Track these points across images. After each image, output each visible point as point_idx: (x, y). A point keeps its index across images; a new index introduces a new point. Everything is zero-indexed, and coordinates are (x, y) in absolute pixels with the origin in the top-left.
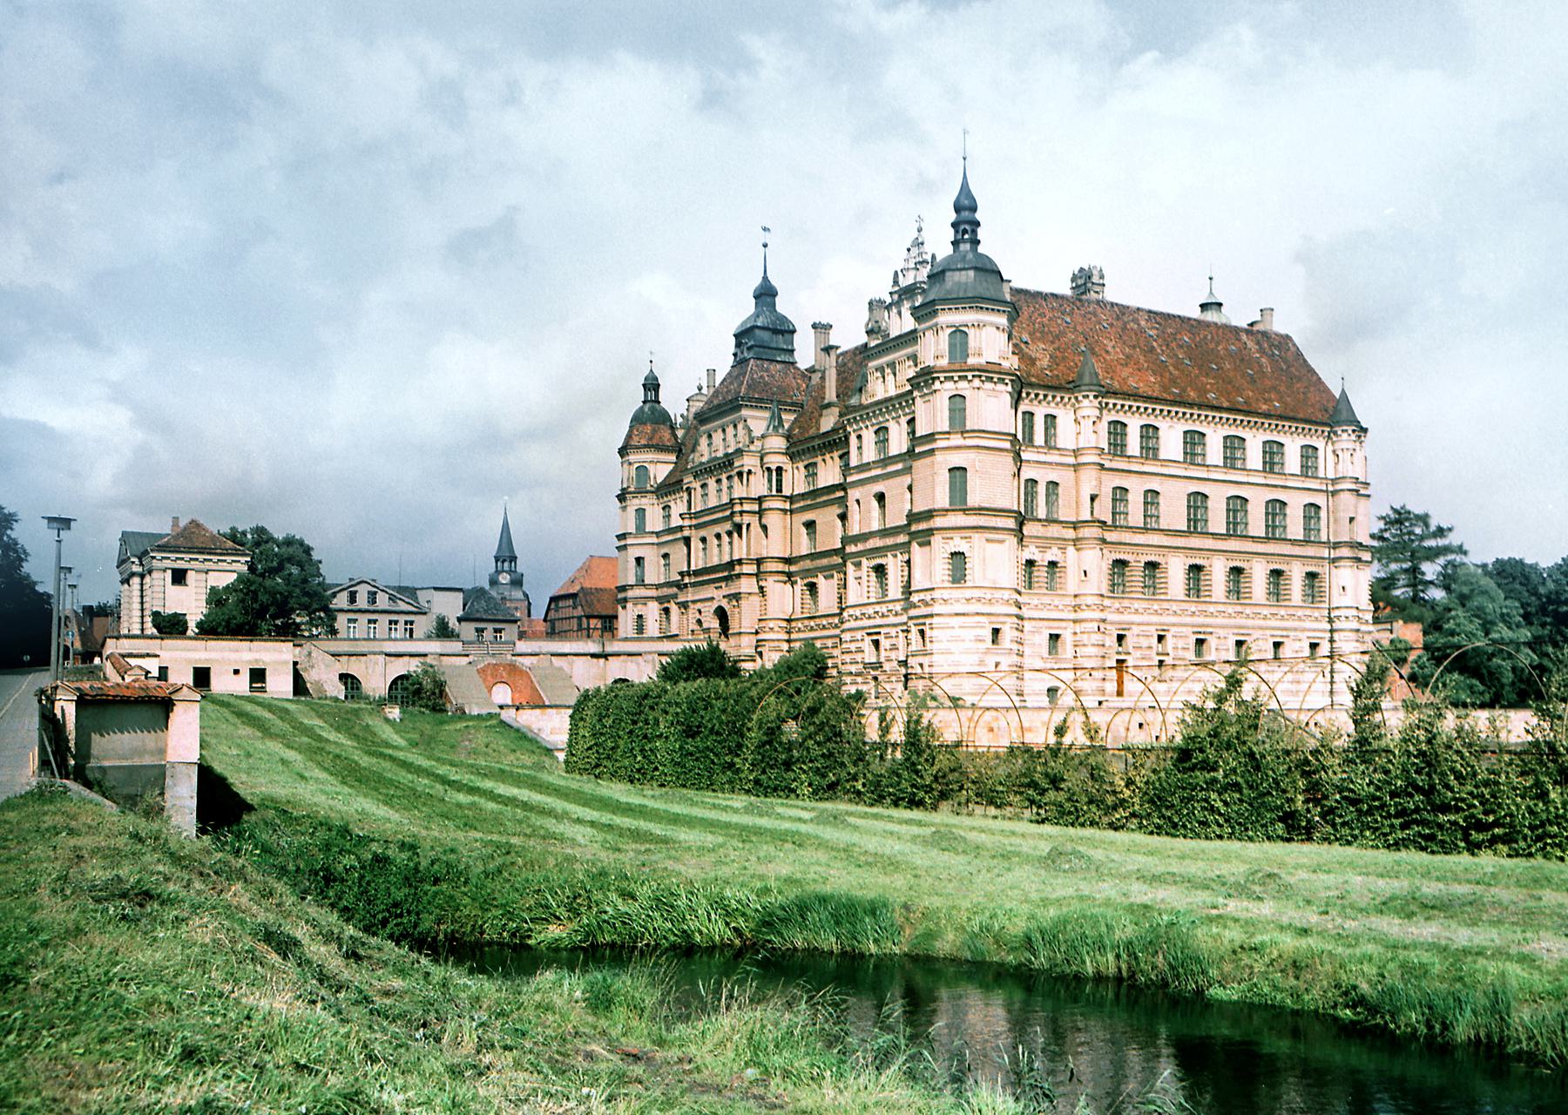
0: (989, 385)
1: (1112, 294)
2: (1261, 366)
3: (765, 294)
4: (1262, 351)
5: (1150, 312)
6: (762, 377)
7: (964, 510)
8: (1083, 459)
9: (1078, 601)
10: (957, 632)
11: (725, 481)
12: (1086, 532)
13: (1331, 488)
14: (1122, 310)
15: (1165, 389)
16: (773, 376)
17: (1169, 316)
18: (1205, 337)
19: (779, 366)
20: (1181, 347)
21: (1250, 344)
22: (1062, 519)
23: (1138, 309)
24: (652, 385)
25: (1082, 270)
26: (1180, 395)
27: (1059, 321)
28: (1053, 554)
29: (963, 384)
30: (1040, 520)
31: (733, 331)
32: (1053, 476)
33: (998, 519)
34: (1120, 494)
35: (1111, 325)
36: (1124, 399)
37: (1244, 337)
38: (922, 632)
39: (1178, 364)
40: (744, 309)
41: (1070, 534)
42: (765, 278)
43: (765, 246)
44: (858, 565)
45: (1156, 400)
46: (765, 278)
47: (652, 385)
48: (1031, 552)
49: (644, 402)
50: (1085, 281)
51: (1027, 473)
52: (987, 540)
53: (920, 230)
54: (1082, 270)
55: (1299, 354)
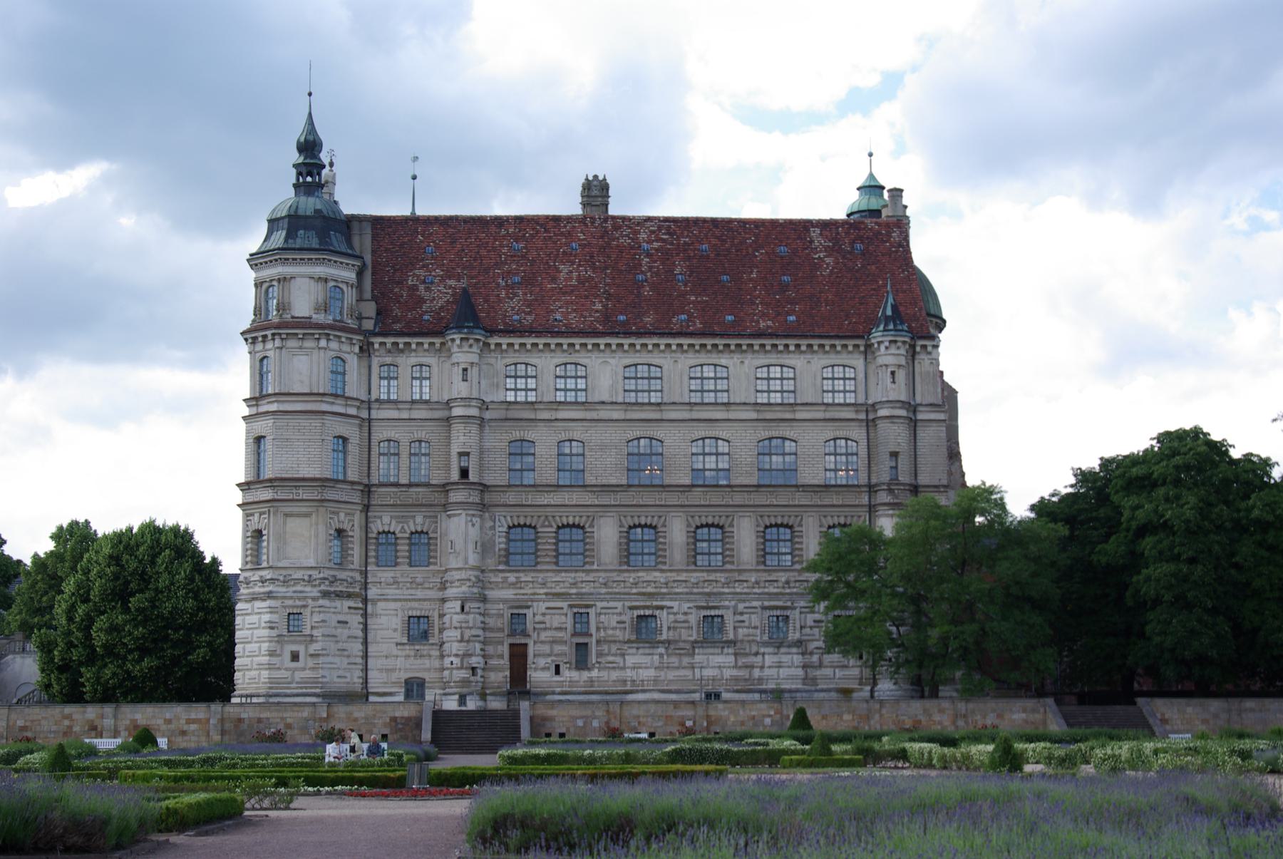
0: (292, 343)
1: (616, 208)
8: (457, 412)
12: (456, 496)
13: (871, 416)
28: (419, 521)
34: (521, 449)
41: (438, 498)
50: (596, 191)
51: (380, 433)
52: (286, 515)
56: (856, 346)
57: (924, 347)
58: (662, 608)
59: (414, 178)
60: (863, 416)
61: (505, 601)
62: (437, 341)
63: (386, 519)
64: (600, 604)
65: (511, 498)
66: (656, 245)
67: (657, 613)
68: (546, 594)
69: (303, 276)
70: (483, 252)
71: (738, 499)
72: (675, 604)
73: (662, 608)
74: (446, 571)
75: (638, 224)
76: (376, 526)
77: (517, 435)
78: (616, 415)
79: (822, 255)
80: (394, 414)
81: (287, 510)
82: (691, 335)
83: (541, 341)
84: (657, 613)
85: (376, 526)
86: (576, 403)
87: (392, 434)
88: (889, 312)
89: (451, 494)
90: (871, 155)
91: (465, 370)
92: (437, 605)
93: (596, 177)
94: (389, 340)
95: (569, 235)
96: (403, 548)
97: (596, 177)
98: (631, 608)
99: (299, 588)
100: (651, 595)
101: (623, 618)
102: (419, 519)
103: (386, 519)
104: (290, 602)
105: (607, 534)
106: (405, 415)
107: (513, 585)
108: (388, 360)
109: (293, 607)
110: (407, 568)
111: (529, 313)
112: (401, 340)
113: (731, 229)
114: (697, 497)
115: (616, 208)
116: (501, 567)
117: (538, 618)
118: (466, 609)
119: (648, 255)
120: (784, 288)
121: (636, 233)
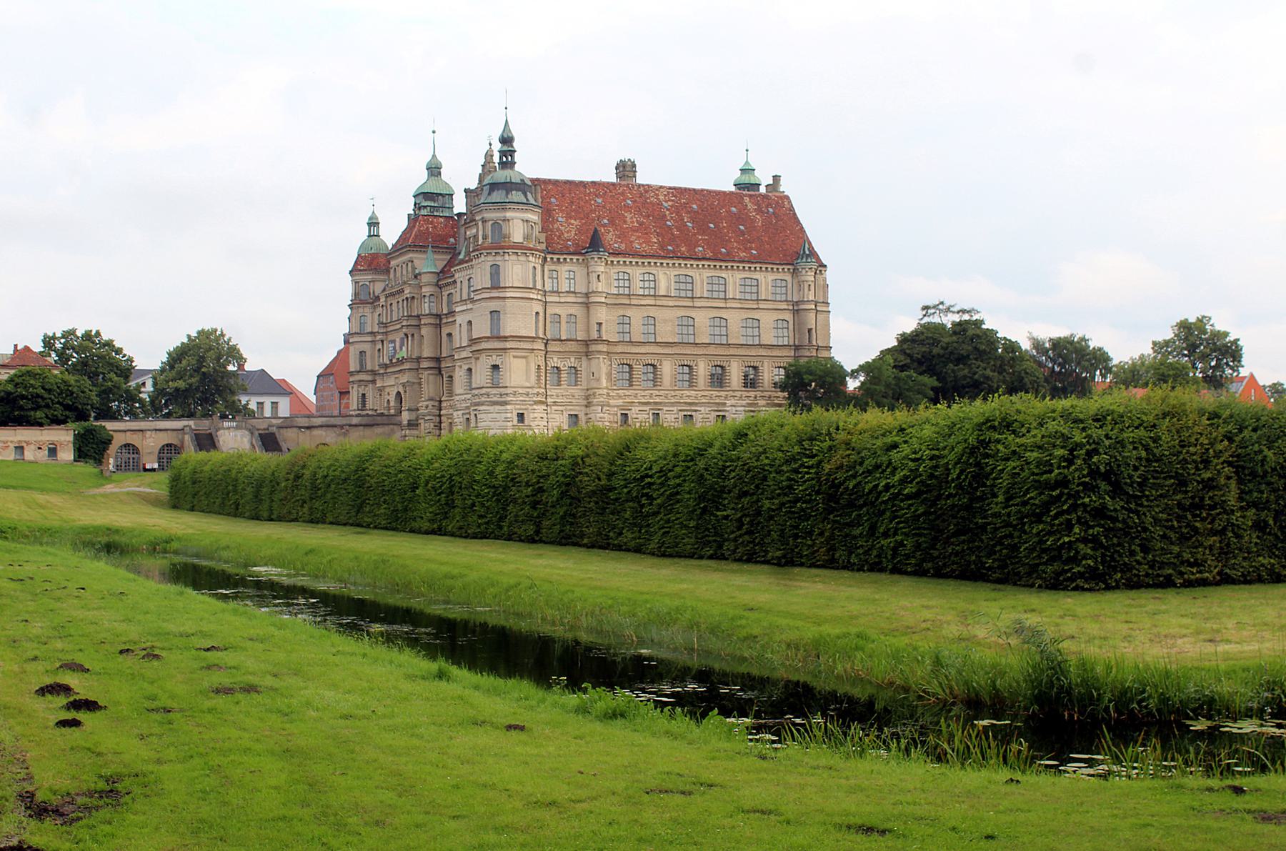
1: (641, 178)
2: (753, 221)
3: (434, 170)
4: (759, 211)
5: (670, 188)
6: (428, 228)
7: (498, 338)
9: (590, 392)
10: (495, 416)
11: (395, 305)
14: (648, 188)
15: (662, 247)
16: (435, 227)
17: (685, 189)
18: (712, 204)
19: (442, 220)
20: (688, 212)
21: (750, 206)
22: (579, 339)
23: (661, 187)
24: (373, 224)
25: (621, 161)
26: (673, 252)
27: (593, 202)
29: (498, 258)
30: (562, 341)
31: (413, 192)
32: (572, 311)
33: (522, 343)
35: (634, 202)
36: (625, 257)
37: (747, 200)
38: (476, 415)
39: (682, 227)
40: (420, 177)
42: (434, 156)
43: (434, 132)
44: (461, 367)
45: (652, 256)
46: (434, 156)
47: (373, 224)
48: (555, 361)
49: (369, 236)
50: (626, 169)
52: (514, 357)
53: (490, 144)
54: (621, 161)
55: (792, 209)
56: (789, 269)
57: (820, 271)
58: (696, 411)
59: (434, 132)
60: (791, 308)
61: (617, 406)
62: (581, 258)
63: (555, 360)
64: (665, 409)
65: (619, 349)
66: (670, 203)
67: (693, 414)
68: (639, 403)
69: (516, 218)
70: (582, 203)
71: (732, 352)
72: (702, 409)
73: (696, 411)
74: (588, 390)
75: (657, 190)
76: (551, 363)
77: (622, 312)
78: (671, 303)
79: (754, 214)
80: (557, 299)
81: (515, 354)
82: (709, 259)
83: (634, 260)
84: (693, 414)
85: (551, 363)
86: (649, 295)
87: (558, 310)
88: (807, 252)
89: (590, 346)
90: (747, 150)
91: (599, 276)
92: (583, 408)
93: (629, 160)
94: (555, 257)
95: (623, 194)
96: (564, 376)
97: (629, 160)
98: (681, 410)
99: (522, 399)
100: (690, 404)
101: (676, 416)
102: (572, 360)
103: (555, 360)
104: (518, 407)
105: (667, 368)
106: (562, 300)
107: (620, 397)
108: (553, 267)
109: (520, 409)
110: (566, 386)
111: (621, 242)
112: (562, 257)
113: (704, 195)
114: (711, 350)
115: (641, 178)
116: (615, 388)
117: (635, 416)
118: (604, 411)
119: (668, 210)
120: (743, 233)
121: (657, 195)
